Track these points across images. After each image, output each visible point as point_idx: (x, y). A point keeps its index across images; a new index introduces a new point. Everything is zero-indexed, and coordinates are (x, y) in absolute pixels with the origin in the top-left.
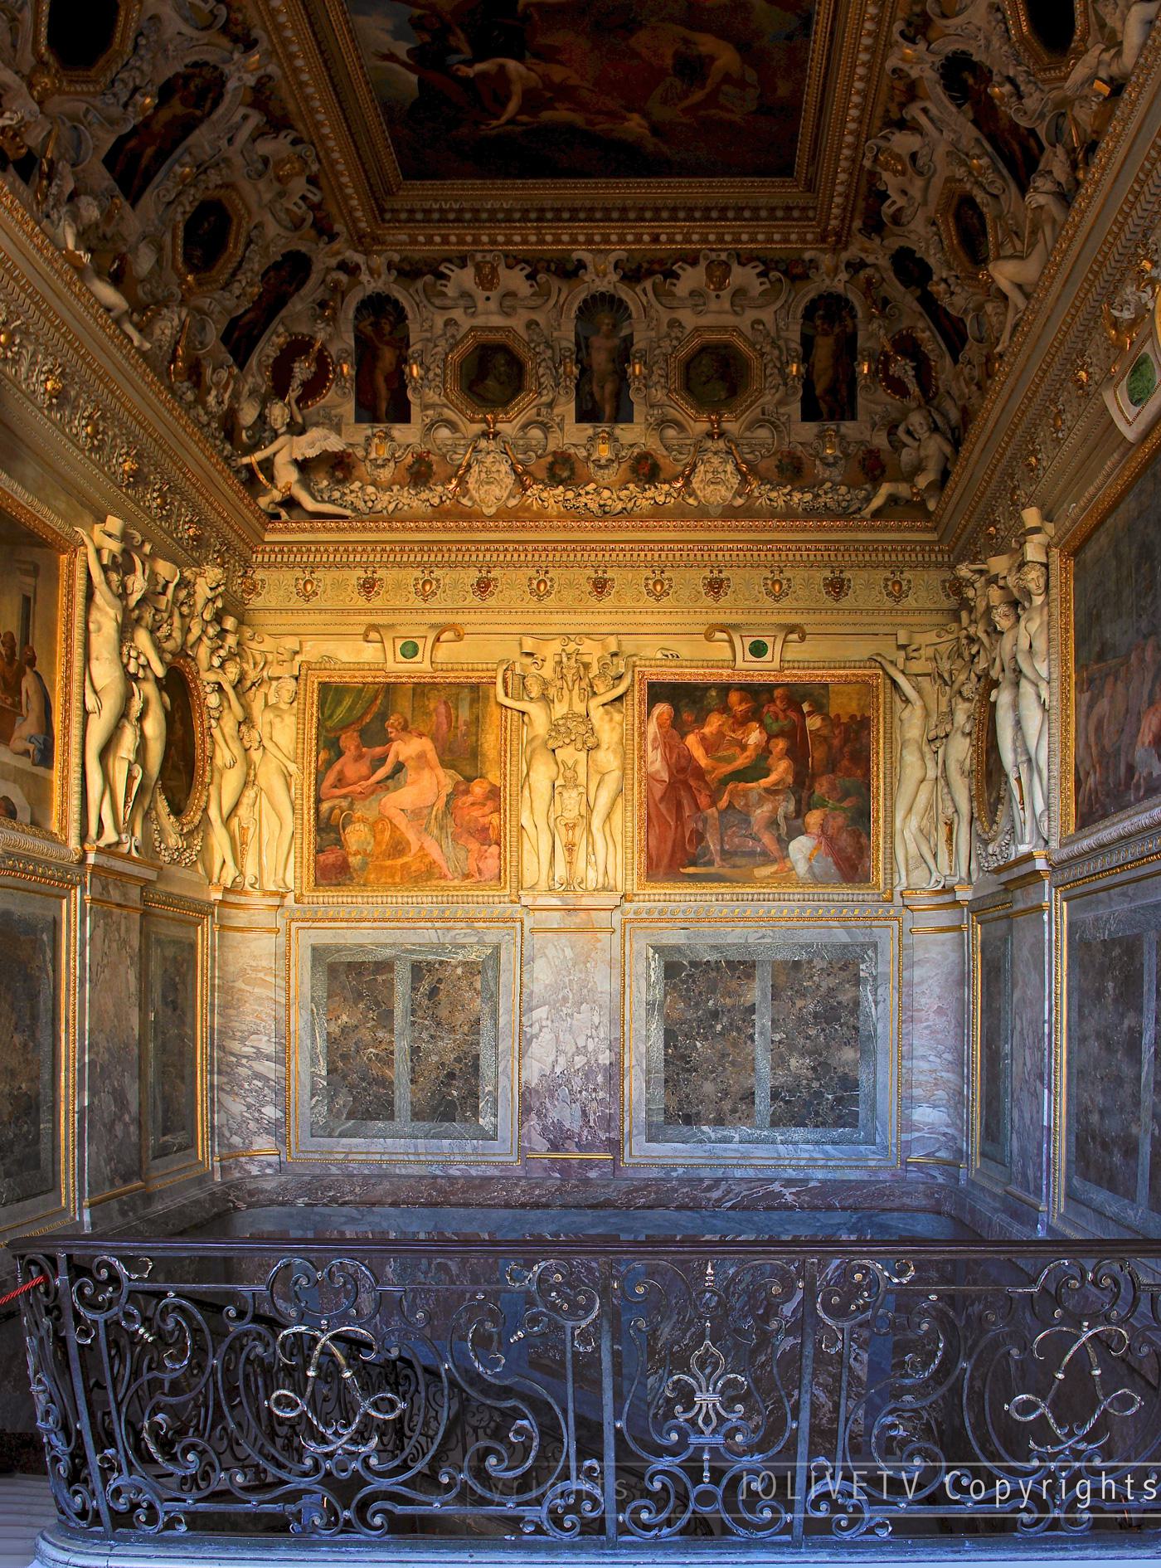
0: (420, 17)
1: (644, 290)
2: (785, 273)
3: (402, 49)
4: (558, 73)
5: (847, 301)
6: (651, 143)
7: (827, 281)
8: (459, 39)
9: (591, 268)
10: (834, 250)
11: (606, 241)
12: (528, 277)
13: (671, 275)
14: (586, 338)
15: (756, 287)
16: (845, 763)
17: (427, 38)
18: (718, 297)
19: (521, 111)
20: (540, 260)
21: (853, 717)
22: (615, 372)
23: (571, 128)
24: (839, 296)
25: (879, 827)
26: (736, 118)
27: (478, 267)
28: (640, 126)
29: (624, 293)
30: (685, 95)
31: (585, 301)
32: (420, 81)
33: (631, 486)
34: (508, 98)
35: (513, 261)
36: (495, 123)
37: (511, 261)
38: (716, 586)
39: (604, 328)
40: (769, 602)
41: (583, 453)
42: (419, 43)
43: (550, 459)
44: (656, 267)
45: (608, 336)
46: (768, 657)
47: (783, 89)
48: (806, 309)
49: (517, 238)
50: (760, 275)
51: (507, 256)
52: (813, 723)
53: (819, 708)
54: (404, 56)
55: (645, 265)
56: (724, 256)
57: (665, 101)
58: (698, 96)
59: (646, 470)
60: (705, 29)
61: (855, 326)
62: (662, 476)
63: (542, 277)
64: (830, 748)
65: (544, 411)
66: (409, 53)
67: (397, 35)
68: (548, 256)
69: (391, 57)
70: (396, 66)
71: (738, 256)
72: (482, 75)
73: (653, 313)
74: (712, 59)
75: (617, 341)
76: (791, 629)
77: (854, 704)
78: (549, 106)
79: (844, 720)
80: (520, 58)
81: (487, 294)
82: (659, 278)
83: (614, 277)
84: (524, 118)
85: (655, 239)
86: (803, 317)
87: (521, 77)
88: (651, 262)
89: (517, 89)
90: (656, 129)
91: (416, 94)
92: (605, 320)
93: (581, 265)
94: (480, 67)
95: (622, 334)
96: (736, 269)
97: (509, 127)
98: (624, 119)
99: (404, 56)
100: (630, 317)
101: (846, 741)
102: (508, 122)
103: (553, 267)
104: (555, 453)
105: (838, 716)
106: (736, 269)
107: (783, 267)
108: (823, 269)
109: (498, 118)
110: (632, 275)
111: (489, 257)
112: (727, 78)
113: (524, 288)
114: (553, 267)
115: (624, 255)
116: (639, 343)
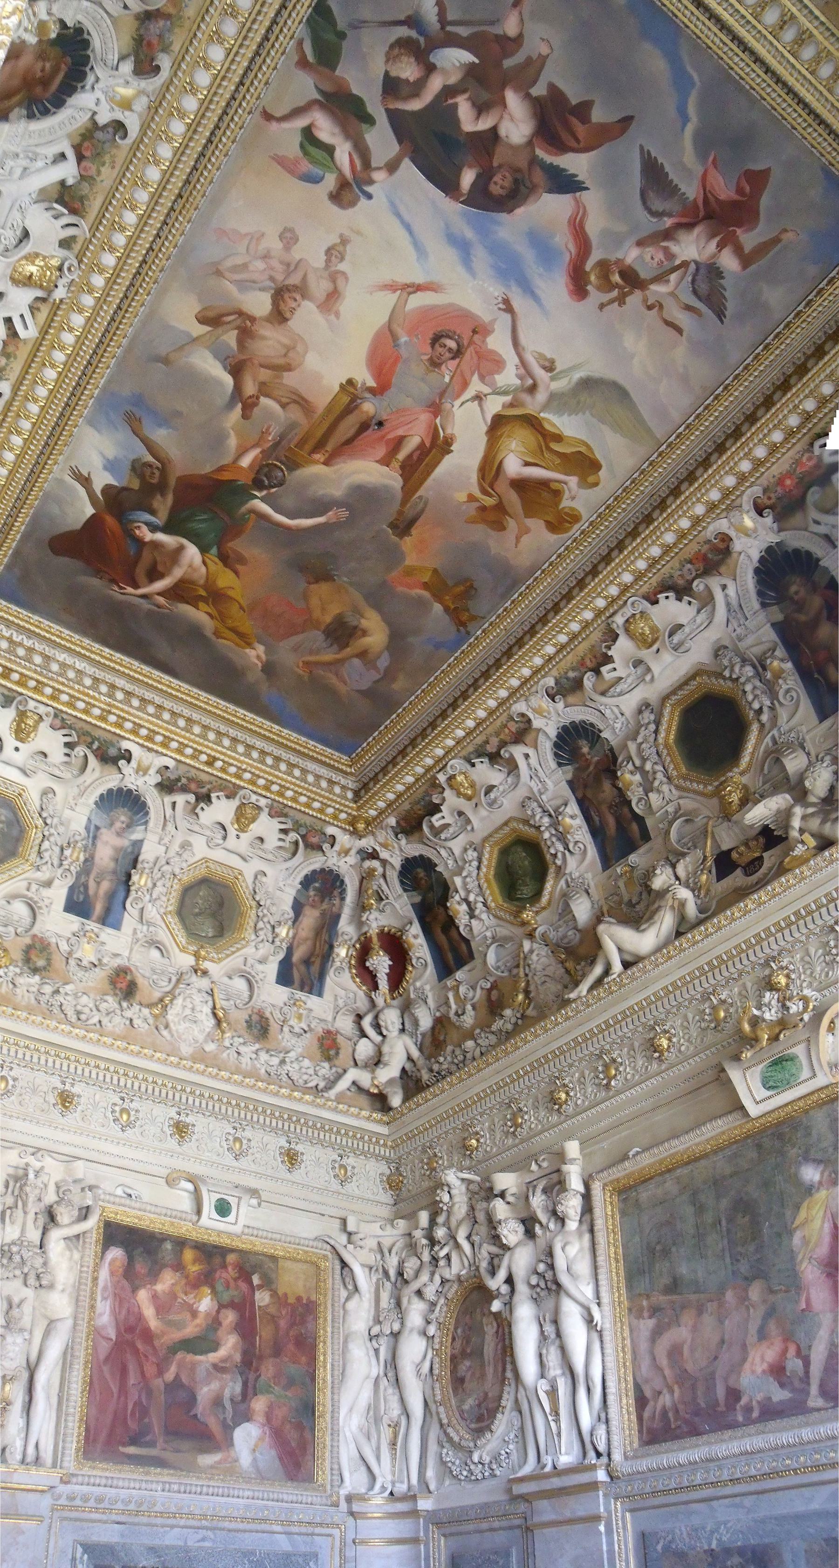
0: (149, 465)
1: (174, 804)
2: (303, 837)
3: (102, 479)
4: (226, 579)
5: (342, 882)
6: (255, 675)
7: (335, 860)
8: (163, 505)
9: (134, 763)
10: (355, 833)
11: (164, 745)
12: (68, 745)
13: (205, 798)
14: (97, 828)
15: (273, 840)
16: (291, 1347)
17: (136, 485)
18: (238, 837)
19: (159, 594)
20: (87, 734)
21: (299, 1299)
22: (114, 872)
23: (195, 632)
24: (338, 876)
25: (323, 1424)
26: (343, 689)
27: (22, 715)
28: (258, 657)
29: (153, 799)
30: (318, 652)
31: (110, 791)
32: (93, 515)
33: (110, 999)
34: (161, 576)
35: (61, 722)
36: (130, 590)
37: (58, 723)
38: (181, 1130)
39: (118, 825)
40: (229, 1159)
41: (64, 947)
42: (124, 483)
43: (28, 940)
44: (193, 786)
45: (119, 834)
46: (231, 1218)
47: (399, 684)
48: (306, 876)
49: (81, 705)
50: (284, 831)
51: (56, 716)
52: (262, 1298)
53: (268, 1283)
54: (98, 487)
55: (184, 781)
56: (263, 802)
57: (295, 649)
58: (328, 657)
59: (123, 985)
60: (377, 606)
61: (341, 907)
62: (138, 997)
63: (80, 751)
64: (277, 1327)
65: (34, 887)
66: (107, 489)
67: (110, 466)
68: (97, 733)
69: (86, 481)
70: (82, 491)
71: (271, 807)
72: (156, 545)
73: (170, 827)
74: (365, 633)
75: (125, 843)
76: (254, 1193)
77: (301, 1284)
78: (194, 601)
79: (291, 1300)
80: (204, 550)
81: (19, 744)
82: (192, 798)
83: (153, 778)
84: (161, 600)
85: (210, 762)
86: (301, 883)
87: (190, 566)
88: (190, 780)
89: (178, 573)
90: (269, 669)
91: (78, 525)
92: (122, 817)
93: (127, 756)
94: (160, 537)
95: (136, 836)
96: (264, 817)
97: (142, 601)
98: (249, 645)
99: (98, 487)
100: (146, 823)
101: (292, 1325)
102: (144, 596)
103: (95, 746)
104: (35, 936)
105: (286, 1295)
106: (264, 817)
107: (303, 831)
108: (337, 847)
109: (136, 586)
110: (167, 786)
111: (42, 710)
112: (362, 655)
113: (57, 754)
114: (95, 746)
115: (171, 763)
116: (148, 853)
